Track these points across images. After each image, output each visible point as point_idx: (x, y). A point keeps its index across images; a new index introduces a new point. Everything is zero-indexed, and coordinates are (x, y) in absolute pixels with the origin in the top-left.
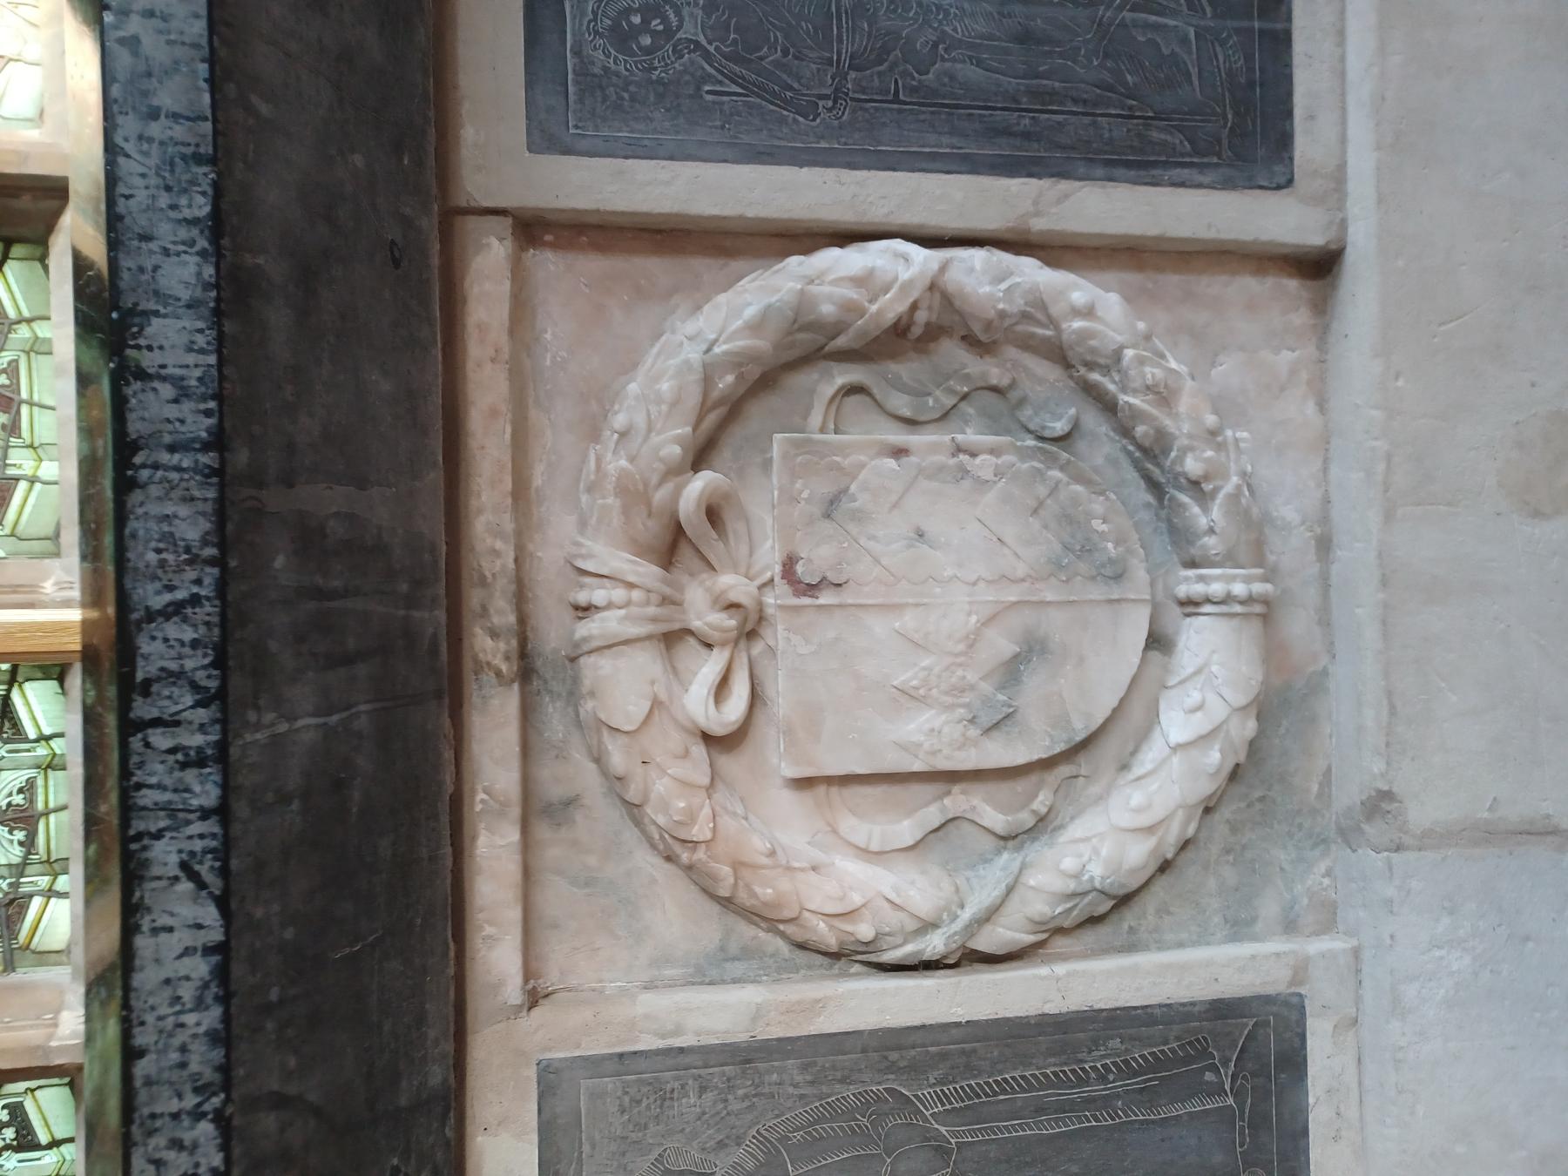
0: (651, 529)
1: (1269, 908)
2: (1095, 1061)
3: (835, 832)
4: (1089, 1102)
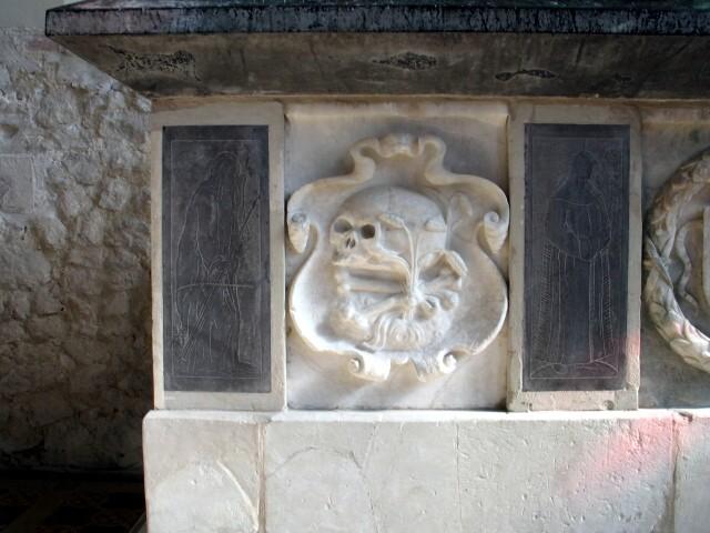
3: (681, 227)
4: (597, 308)
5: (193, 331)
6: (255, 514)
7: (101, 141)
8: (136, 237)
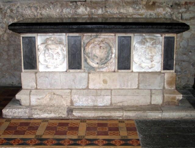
0: (103, 41)
1: (85, 68)
2: (79, 60)
5: (27, 62)
6: (35, 85)
7: (6, 19)
8: (14, 39)
